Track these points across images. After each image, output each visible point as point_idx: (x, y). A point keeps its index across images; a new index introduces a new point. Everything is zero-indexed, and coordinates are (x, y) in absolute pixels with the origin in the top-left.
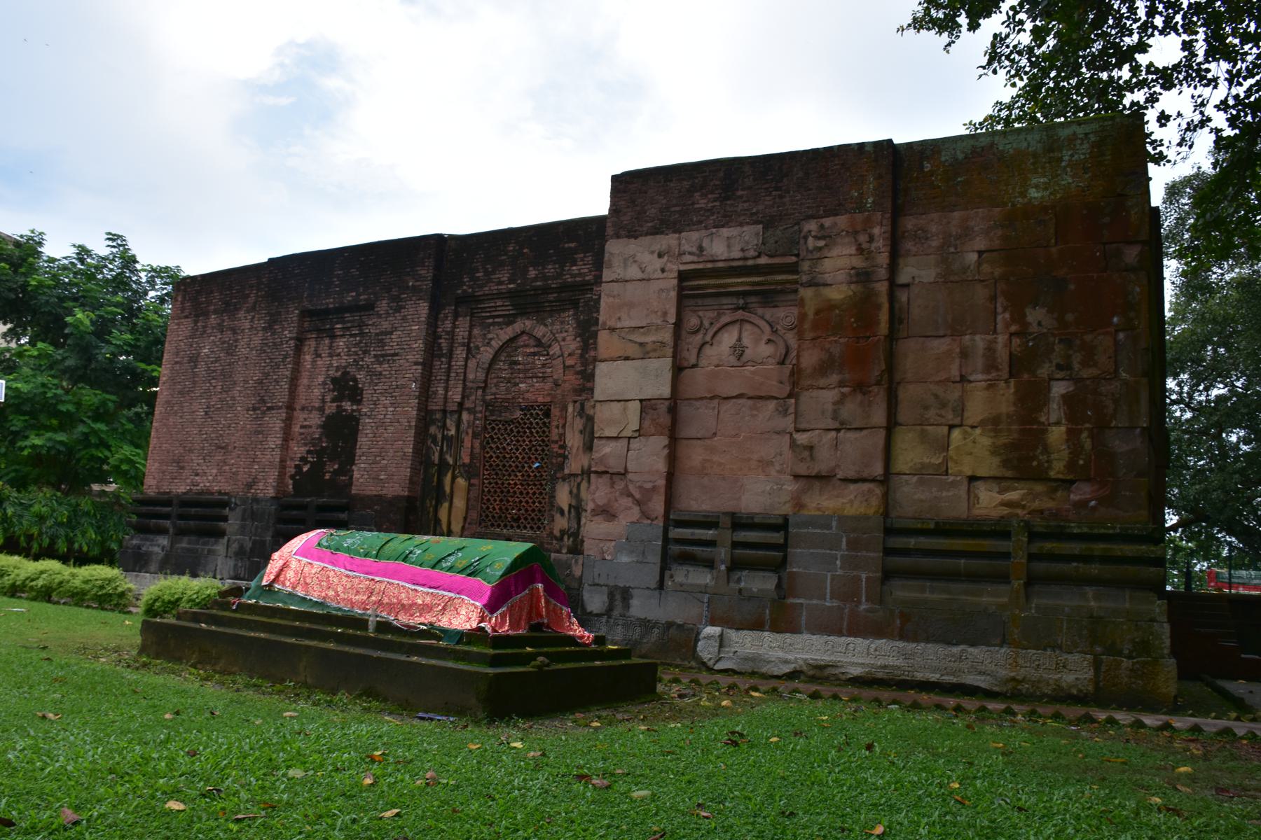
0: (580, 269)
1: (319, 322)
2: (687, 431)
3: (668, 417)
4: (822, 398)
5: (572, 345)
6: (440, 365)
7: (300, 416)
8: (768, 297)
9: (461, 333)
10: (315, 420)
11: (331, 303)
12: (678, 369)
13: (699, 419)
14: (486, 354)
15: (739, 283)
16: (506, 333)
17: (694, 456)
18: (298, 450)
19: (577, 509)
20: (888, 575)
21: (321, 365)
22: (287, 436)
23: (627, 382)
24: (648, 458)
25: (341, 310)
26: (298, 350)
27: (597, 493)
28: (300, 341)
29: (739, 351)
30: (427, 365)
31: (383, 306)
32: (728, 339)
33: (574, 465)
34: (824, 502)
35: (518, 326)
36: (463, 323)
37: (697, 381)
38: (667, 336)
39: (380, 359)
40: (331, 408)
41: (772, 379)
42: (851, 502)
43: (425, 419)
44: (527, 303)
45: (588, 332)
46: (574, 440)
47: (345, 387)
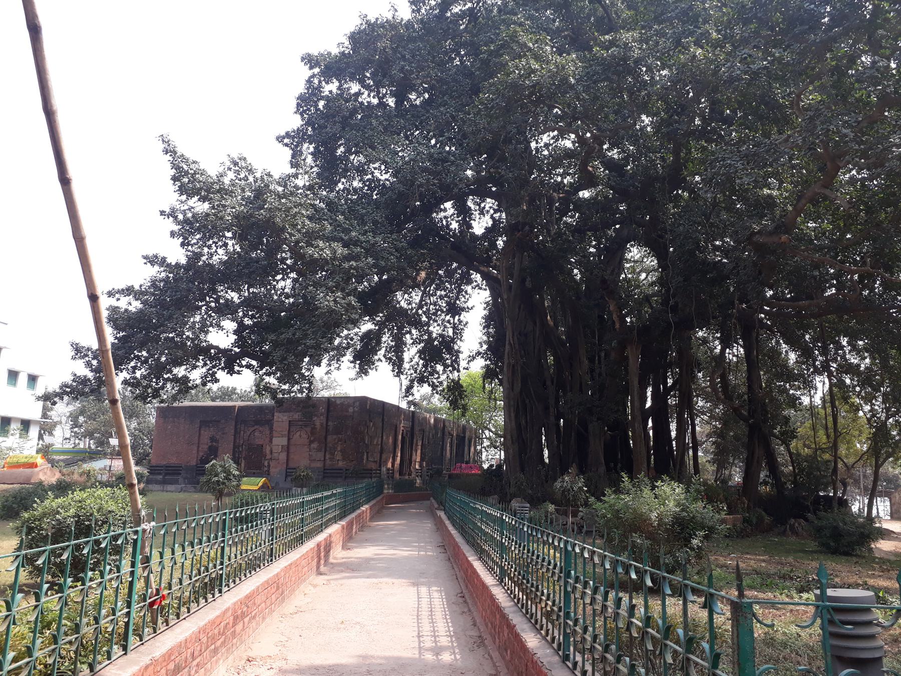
0: (269, 417)
1: (204, 424)
3: (287, 449)
4: (315, 445)
5: (268, 432)
7: (201, 446)
8: (306, 426)
9: (242, 428)
12: (289, 439)
13: (292, 449)
14: (249, 433)
15: (300, 423)
17: (292, 456)
18: (201, 454)
19: (269, 466)
20: (324, 477)
21: (206, 434)
22: (198, 451)
23: (280, 441)
24: (283, 456)
27: (272, 464)
31: (223, 421)
32: (298, 433)
34: (314, 465)
35: (256, 427)
37: (292, 441)
39: (223, 434)
41: (307, 441)
42: (319, 465)
44: (257, 422)
45: (271, 429)
46: (268, 452)
47: (213, 439)
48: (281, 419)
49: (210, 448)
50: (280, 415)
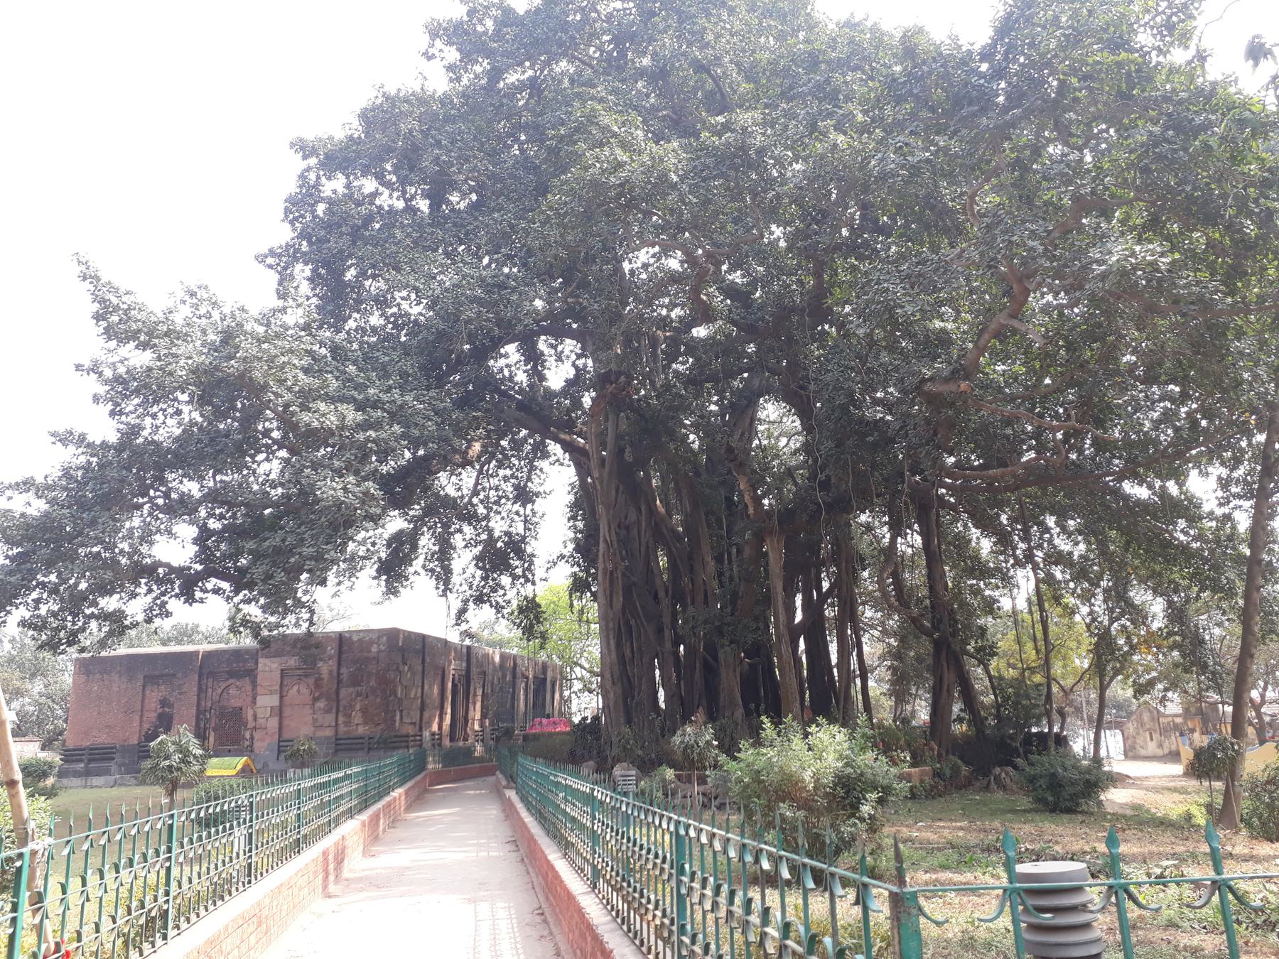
0: (250, 665)
1: (150, 680)
2: (285, 714)
3: (280, 712)
4: (321, 704)
5: (249, 688)
6: (203, 695)
7: (146, 714)
8: (306, 676)
9: (210, 684)
10: (154, 715)
11: (157, 673)
12: (281, 697)
13: (287, 712)
15: (299, 672)
16: (223, 685)
17: (286, 722)
18: (146, 726)
19: (252, 738)
20: (337, 751)
21: (154, 696)
22: (141, 722)
23: (267, 701)
24: (273, 723)
25: (161, 676)
26: (144, 690)
27: (257, 735)
28: (144, 687)
29: (299, 691)
30: (198, 695)
31: (179, 675)
32: (296, 688)
33: (251, 725)
34: (321, 733)
35: (231, 681)
36: (211, 680)
38: (277, 688)
39: (180, 694)
40: (160, 711)
41: (308, 699)
42: (329, 732)
43: (199, 713)
44: (232, 674)
45: (254, 684)
46: (250, 718)
47: (164, 703)
48: (269, 668)
49: (160, 716)
50: (267, 661)
